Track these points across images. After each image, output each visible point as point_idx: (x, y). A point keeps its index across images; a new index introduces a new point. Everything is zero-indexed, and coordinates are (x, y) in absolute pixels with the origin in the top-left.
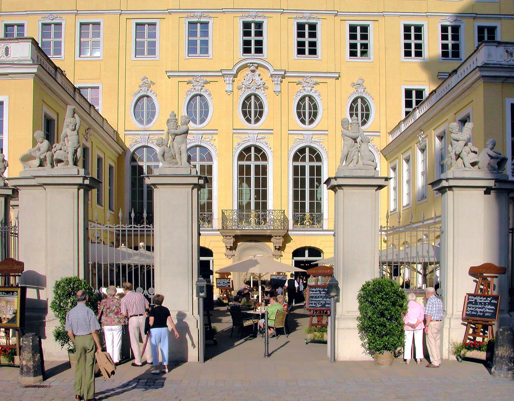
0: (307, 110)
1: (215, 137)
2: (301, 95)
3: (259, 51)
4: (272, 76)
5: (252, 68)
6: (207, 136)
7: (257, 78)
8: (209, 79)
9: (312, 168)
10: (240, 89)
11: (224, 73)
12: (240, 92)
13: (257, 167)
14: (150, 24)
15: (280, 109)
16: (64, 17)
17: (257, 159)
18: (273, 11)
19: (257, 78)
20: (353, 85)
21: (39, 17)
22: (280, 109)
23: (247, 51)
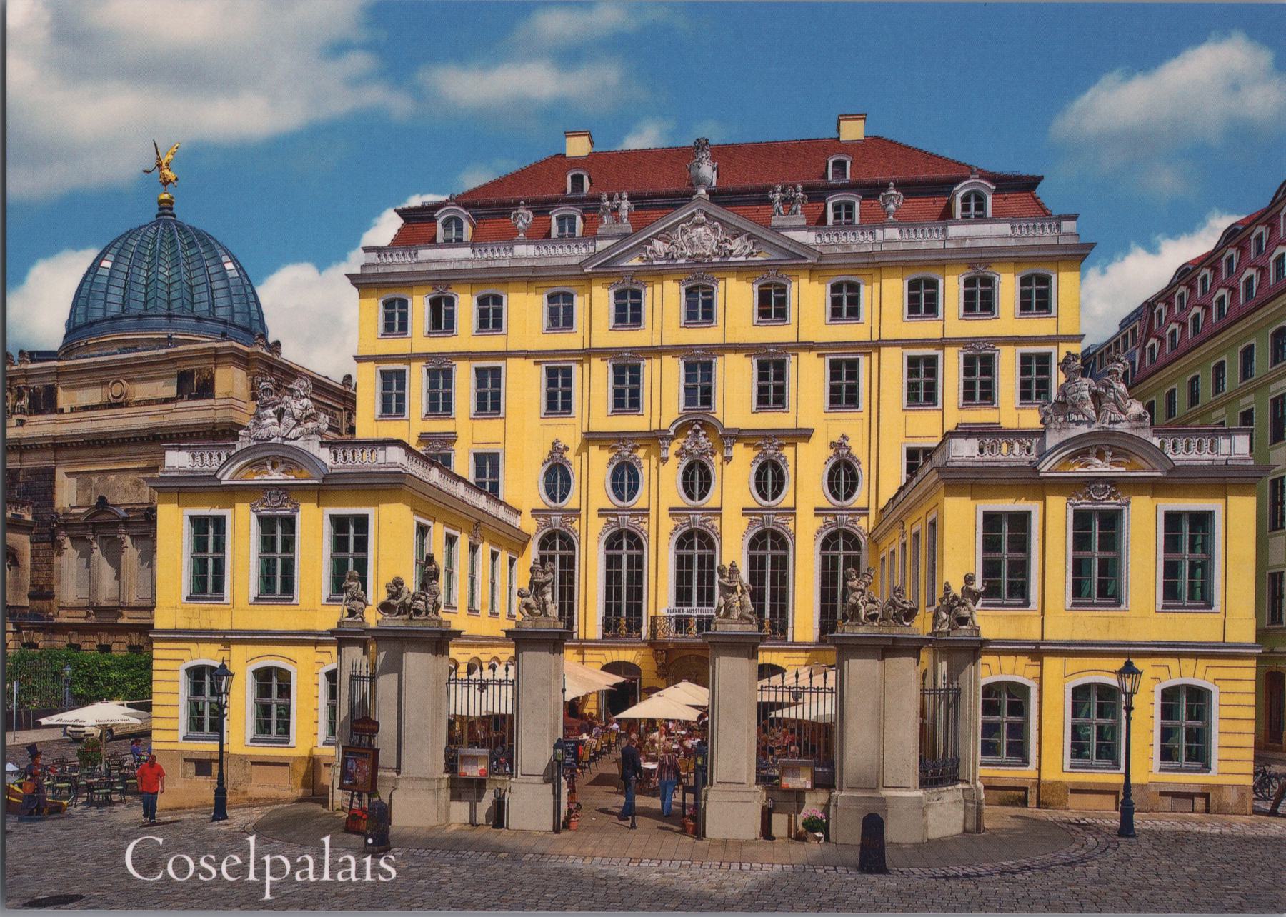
0: (770, 478)
1: (646, 519)
2: (761, 461)
3: (707, 401)
4: (721, 437)
5: (698, 427)
7: (702, 440)
9: (774, 558)
10: (678, 455)
13: (701, 558)
14: (563, 368)
15: (735, 479)
17: (700, 547)
19: (702, 440)
20: (833, 445)
22: (735, 479)
23: (690, 400)
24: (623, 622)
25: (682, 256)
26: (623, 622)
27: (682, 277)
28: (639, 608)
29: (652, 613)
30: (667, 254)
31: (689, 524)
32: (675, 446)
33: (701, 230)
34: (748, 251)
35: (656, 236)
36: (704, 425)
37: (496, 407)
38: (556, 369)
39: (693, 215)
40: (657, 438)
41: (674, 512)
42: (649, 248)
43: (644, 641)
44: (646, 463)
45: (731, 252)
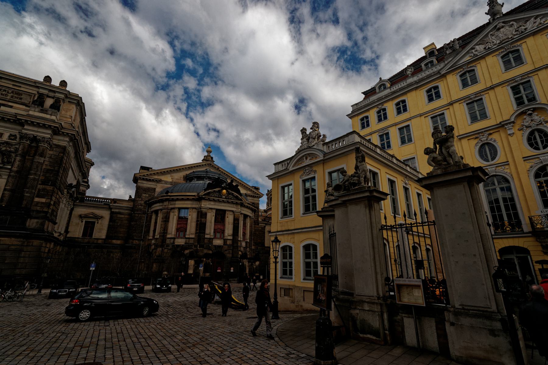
1: (507, 167)
5: (530, 112)
6: (500, 168)
7: (536, 118)
8: (491, 132)
11: (503, 123)
12: (521, 132)
14: (439, 115)
16: (389, 129)
18: (536, 70)
19: (536, 118)
21: (377, 133)
24: (506, 223)
25: (494, 45)
26: (506, 223)
27: (497, 53)
28: (516, 215)
29: (527, 215)
30: (485, 48)
31: (542, 162)
32: (517, 127)
33: (502, 30)
34: (537, 24)
35: (477, 44)
36: (534, 110)
37: (410, 140)
38: (436, 116)
39: (496, 26)
40: (503, 126)
41: (526, 159)
42: (473, 51)
43: (529, 233)
44: (498, 139)
45: (526, 29)
